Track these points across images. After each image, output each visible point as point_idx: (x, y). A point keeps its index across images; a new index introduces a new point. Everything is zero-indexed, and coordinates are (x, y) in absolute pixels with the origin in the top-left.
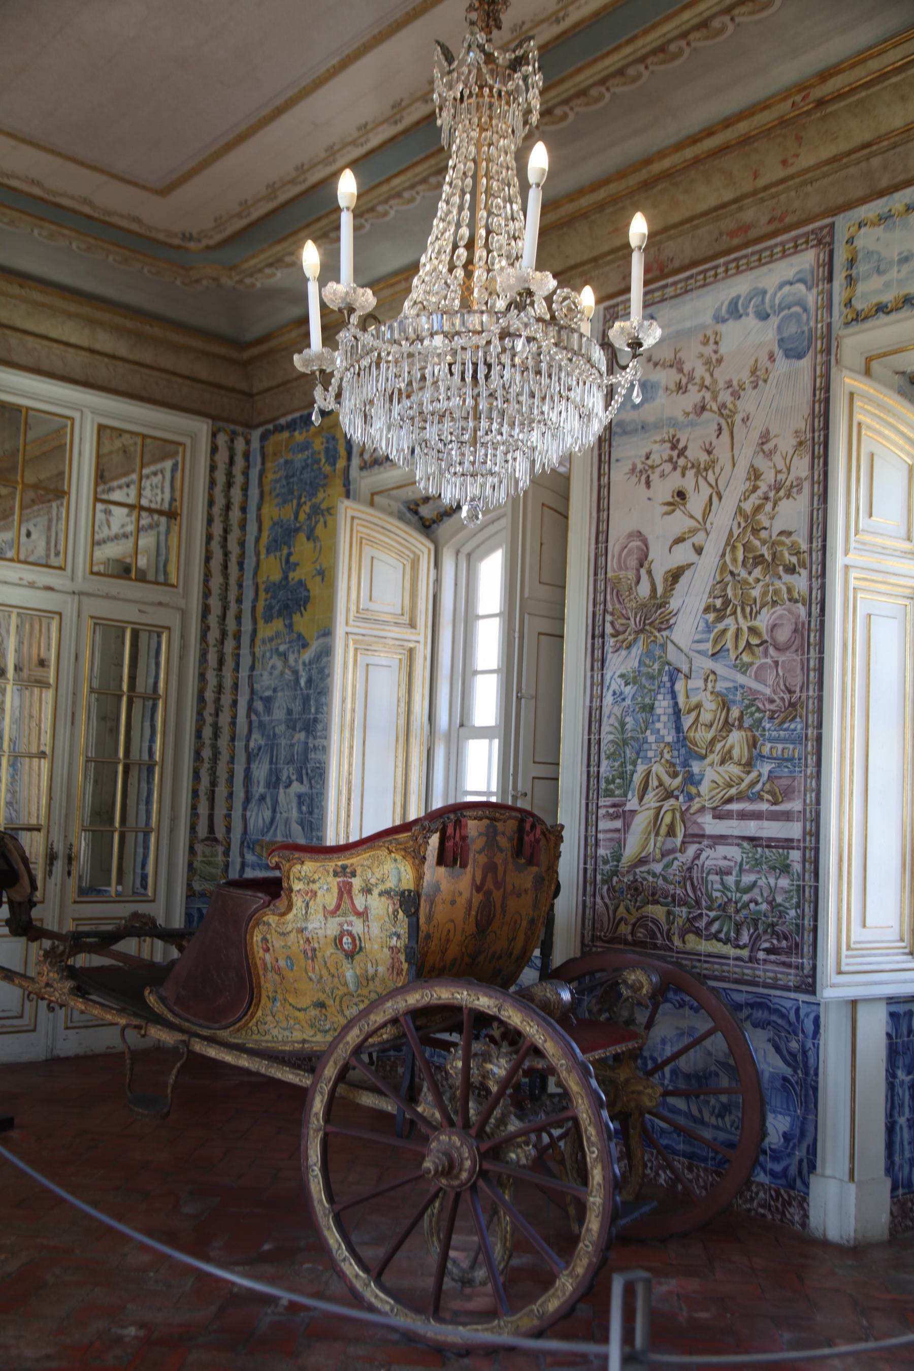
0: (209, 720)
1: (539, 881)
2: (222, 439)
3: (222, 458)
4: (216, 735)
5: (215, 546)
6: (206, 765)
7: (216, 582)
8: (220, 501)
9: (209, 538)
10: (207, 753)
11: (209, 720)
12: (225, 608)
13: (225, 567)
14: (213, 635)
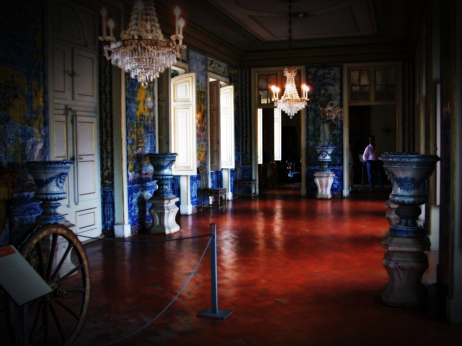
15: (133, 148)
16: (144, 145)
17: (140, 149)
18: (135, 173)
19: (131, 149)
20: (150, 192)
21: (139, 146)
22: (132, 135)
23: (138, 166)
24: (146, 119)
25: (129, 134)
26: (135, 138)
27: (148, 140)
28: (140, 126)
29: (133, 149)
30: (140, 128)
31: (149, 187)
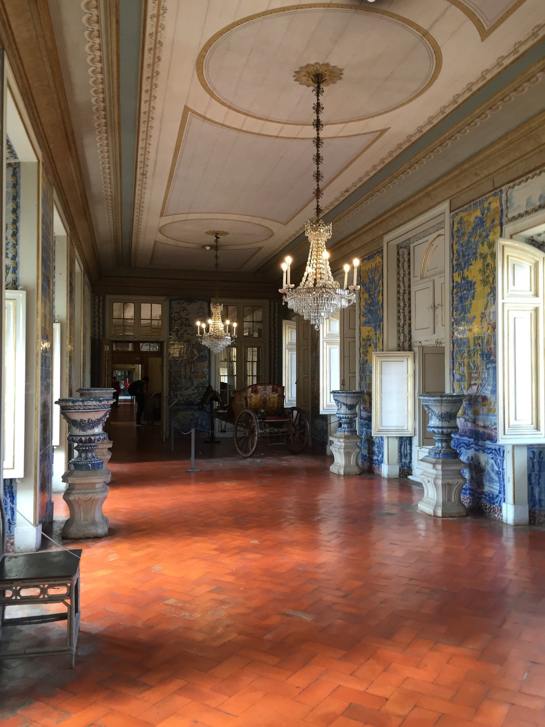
0: (272, 365)
1: (279, 396)
2: (272, 303)
3: (272, 307)
4: (274, 369)
5: (272, 327)
6: (272, 376)
7: (272, 336)
8: (272, 317)
9: (270, 325)
10: (272, 373)
11: (272, 365)
12: (275, 341)
13: (274, 331)
14: (273, 347)
15: (463, 386)
16: (481, 382)
17: (475, 388)
18: (465, 421)
19: (459, 387)
20: (492, 458)
21: (473, 383)
22: (461, 368)
23: (470, 412)
24: (485, 341)
25: (456, 366)
26: (466, 372)
27: (489, 374)
28: (475, 354)
29: (463, 387)
30: (473, 358)
31: (490, 449)
